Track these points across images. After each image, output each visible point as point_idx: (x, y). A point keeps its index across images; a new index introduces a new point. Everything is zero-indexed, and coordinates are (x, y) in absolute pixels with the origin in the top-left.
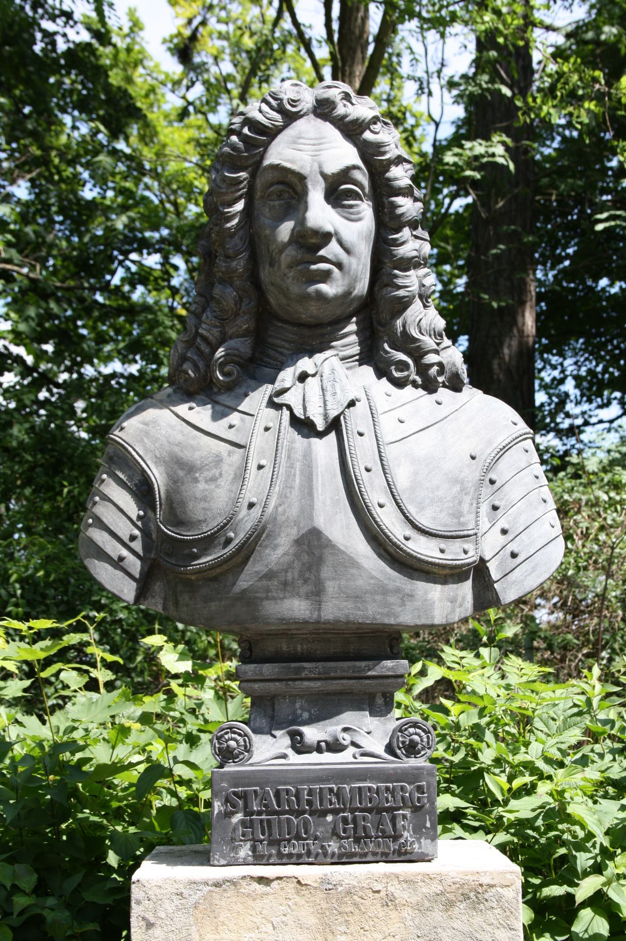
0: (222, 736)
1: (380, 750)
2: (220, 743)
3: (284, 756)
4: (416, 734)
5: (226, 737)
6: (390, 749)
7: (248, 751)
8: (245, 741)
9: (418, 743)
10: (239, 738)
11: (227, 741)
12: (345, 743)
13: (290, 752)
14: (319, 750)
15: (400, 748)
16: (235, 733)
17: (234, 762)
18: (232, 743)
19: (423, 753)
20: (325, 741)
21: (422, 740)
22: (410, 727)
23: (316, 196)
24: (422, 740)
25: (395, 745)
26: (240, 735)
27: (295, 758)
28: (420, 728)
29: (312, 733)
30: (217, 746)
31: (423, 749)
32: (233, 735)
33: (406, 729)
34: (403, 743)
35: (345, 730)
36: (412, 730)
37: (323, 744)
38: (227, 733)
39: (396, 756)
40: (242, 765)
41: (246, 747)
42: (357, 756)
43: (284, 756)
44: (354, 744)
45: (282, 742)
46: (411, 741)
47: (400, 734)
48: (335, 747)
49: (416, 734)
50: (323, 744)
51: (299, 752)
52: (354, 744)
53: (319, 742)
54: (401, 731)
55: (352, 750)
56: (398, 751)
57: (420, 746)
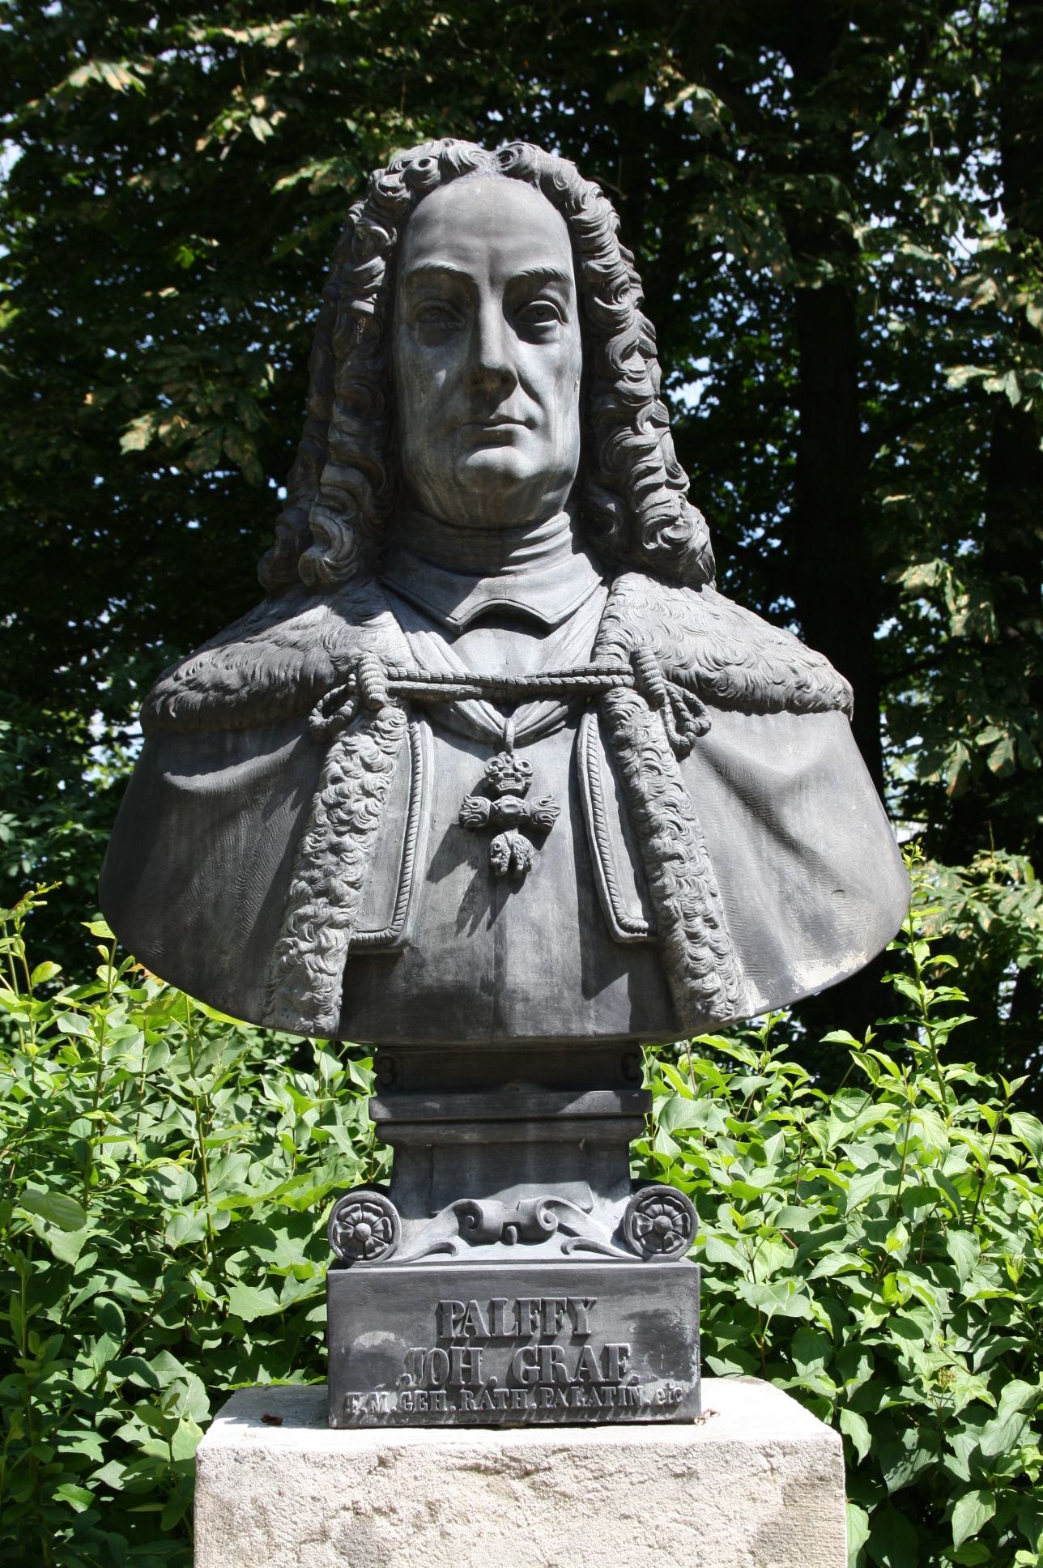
0: (348, 1214)
1: (604, 1237)
3: (448, 1248)
5: (355, 1215)
6: (620, 1237)
7: (390, 1242)
8: (385, 1224)
9: (667, 1229)
10: (374, 1218)
11: (356, 1223)
12: (548, 1227)
13: (459, 1242)
14: (506, 1239)
15: (638, 1239)
16: (369, 1209)
17: (365, 1258)
18: (364, 1227)
19: (676, 1243)
20: (517, 1224)
21: (674, 1224)
22: (654, 1202)
23: (492, 312)
24: (674, 1224)
26: (376, 1213)
27: (464, 1250)
28: (670, 1203)
29: (492, 1210)
30: (340, 1230)
32: (367, 1214)
33: (648, 1206)
35: (550, 1205)
36: (657, 1207)
37: (513, 1229)
39: (629, 1248)
41: (386, 1232)
42: (569, 1249)
43: (448, 1248)
44: (563, 1229)
45: (444, 1226)
46: (658, 1225)
48: (532, 1233)
50: (513, 1229)
51: (474, 1242)
52: (563, 1229)
53: (506, 1225)
55: (559, 1239)
56: (637, 1245)
57: (670, 1234)
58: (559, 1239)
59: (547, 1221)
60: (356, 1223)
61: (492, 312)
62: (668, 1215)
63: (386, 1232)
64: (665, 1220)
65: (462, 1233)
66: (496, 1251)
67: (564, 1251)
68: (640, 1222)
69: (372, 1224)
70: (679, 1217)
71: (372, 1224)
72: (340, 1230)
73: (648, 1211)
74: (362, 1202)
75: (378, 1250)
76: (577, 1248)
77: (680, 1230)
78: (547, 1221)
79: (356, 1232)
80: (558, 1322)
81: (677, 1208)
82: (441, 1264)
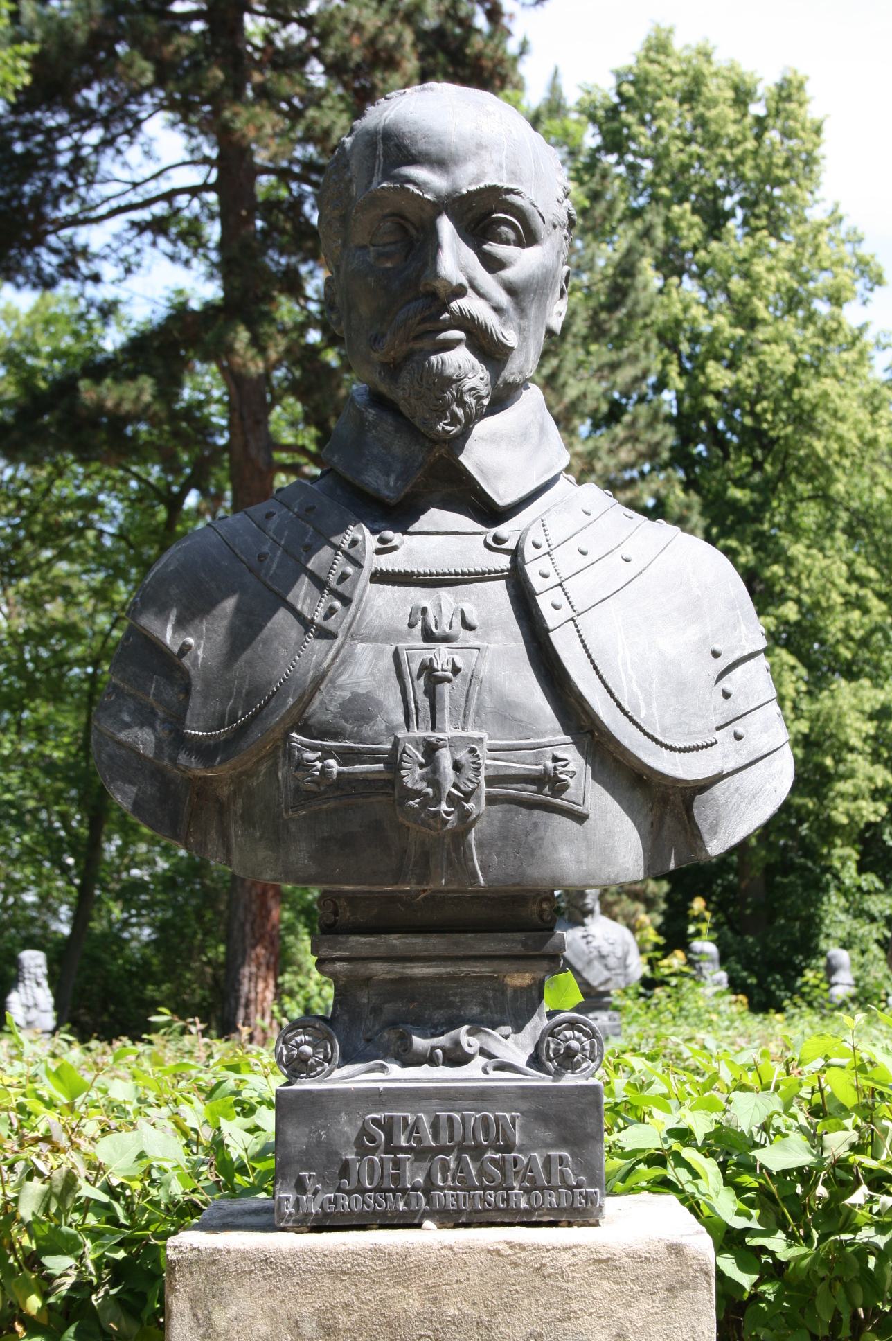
1: (522, 1060)
2: (289, 1050)
4: (574, 1038)
5: (298, 1039)
6: (536, 1061)
14: (432, 1061)
15: (551, 1060)
19: (584, 1065)
22: (566, 1029)
24: (583, 1049)
28: (580, 1030)
30: (285, 1052)
33: (560, 1032)
36: (568, 1034)
37: (439, 1052)
44: (483, 1052)
48: (456, 1058)
49: (574, 1038)
50: (439, 1052)
52: (483, 1052)
55: (480, 1061)
57: (579, 1056)
58: (480, 1061)
59: (470, 1046)
60: (298, 1045)
67: (485, 1072)
68: (552, 1046)
70: (587, 1044)
73: (561, 1037)
75: (319, 1069)
78: (470, 1046)
79: (301, 1053)
81: (586, 1034)
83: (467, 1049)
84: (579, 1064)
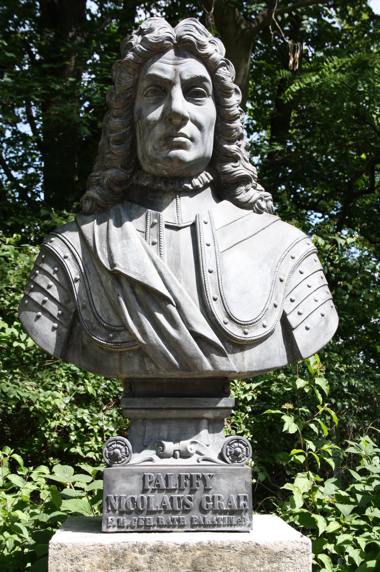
0: (111, 446)
1: (215, 456)
3: (151, 460)
5: (113, 446)
6: (221, 456)
7: (127, 456)
8: (126, 449)
9: (239, 453)
14: (174, 456)
15: (228, 456)
16: (119, 443)
17: (118, 463)
18: (117, 451)
19: (243, 459)
20: (179, 451)
21: (242, 451)
23: (177, 92)
24: (242, 451)
25: (224, 453)
26: (122, 445)
27: (158, 461)
28: (241, 443)
29: (169, 446)
30: (107, 452)
31: (243, 457)
32: (119, 446)
33: (232, 444)
34: (230, 452)
36: (236, 444)
37: (177, 453)
38: (114, 444)
40: (124, 466)
41: (126, 453)
43: (151, 460)
44: (198, 453)
46: (236, 451)
47: (228, 447)
48: (185, 455)
49: (239, 447)
50: (177, 453)
51: (161, 457)
52: (198, 453)
53: (175, 451)
54: (229, 445)
55: (196, 456)
57: (241, 455)
59: (191, 449)
61: (177, 92)
62: (240, 448)
63: (126, 453)
64: (239, 450)
65: (157, 454)
66: (171, 461)
67: (198, 462)
68: (229, 450)
69: (120, 449)
71: (120, 449)
72: (107, 452)
73: (232, 446)
74: (116, 440)
75: (123, 460)
76: (204, 460)
77: (245, 453)
78: (191, 449)
80: (197, 483)
82: (147, 466)
83: (191, 452)
84: (240, 459)
